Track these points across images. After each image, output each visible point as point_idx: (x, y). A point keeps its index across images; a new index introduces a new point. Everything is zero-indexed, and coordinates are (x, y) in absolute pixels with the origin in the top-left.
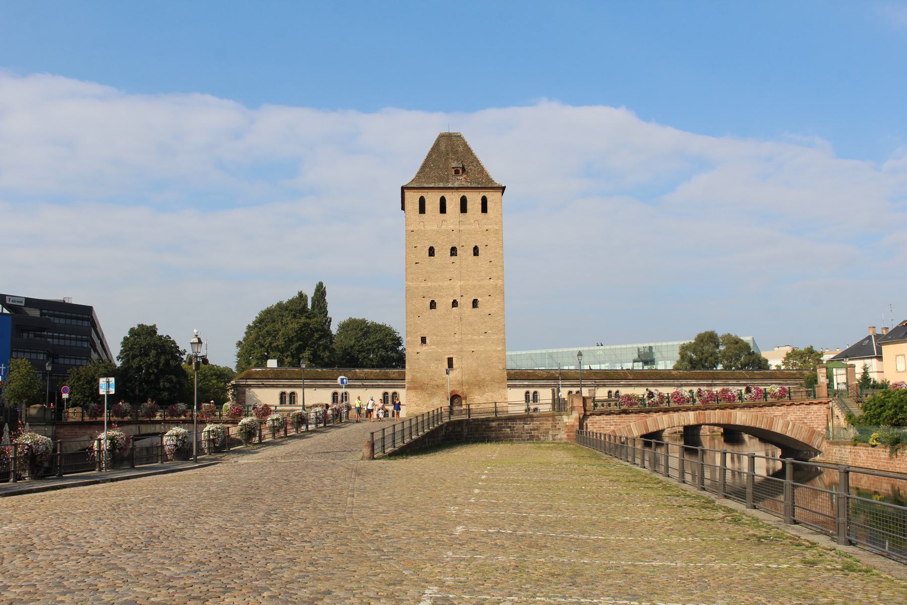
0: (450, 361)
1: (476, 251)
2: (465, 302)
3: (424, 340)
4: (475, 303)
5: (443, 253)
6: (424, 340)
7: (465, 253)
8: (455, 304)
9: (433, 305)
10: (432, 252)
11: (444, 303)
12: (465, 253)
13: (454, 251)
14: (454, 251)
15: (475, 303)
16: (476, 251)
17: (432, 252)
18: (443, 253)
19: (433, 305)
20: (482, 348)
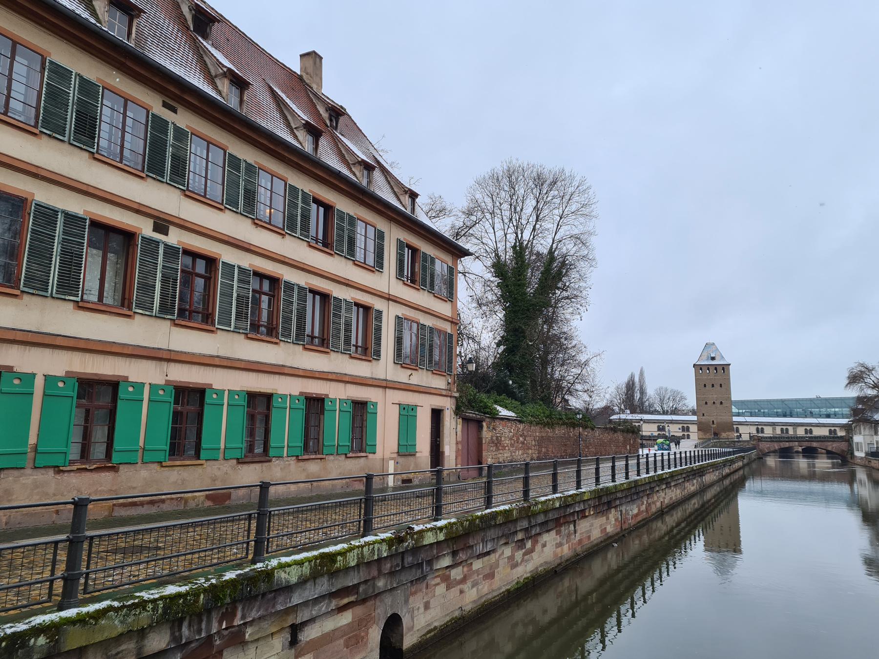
0: (713, 421)
1: (721, 385)
2: (718, 402)
3: (703, 415)
4: (721, 403)
5: (709, 387)
6: (703, 415)
7: (717, 387)
8: (714, 403)
9: (706, 403)
10: (705, 386)
11: (710, 403)
12: (717, 387)
13: (713, 386)
14: (713, 386)
15: (721, 403)
16: (721, 385)
17: (705, 386)
18: (709, 387)
19: (706, 403)
20: (724, 418)
